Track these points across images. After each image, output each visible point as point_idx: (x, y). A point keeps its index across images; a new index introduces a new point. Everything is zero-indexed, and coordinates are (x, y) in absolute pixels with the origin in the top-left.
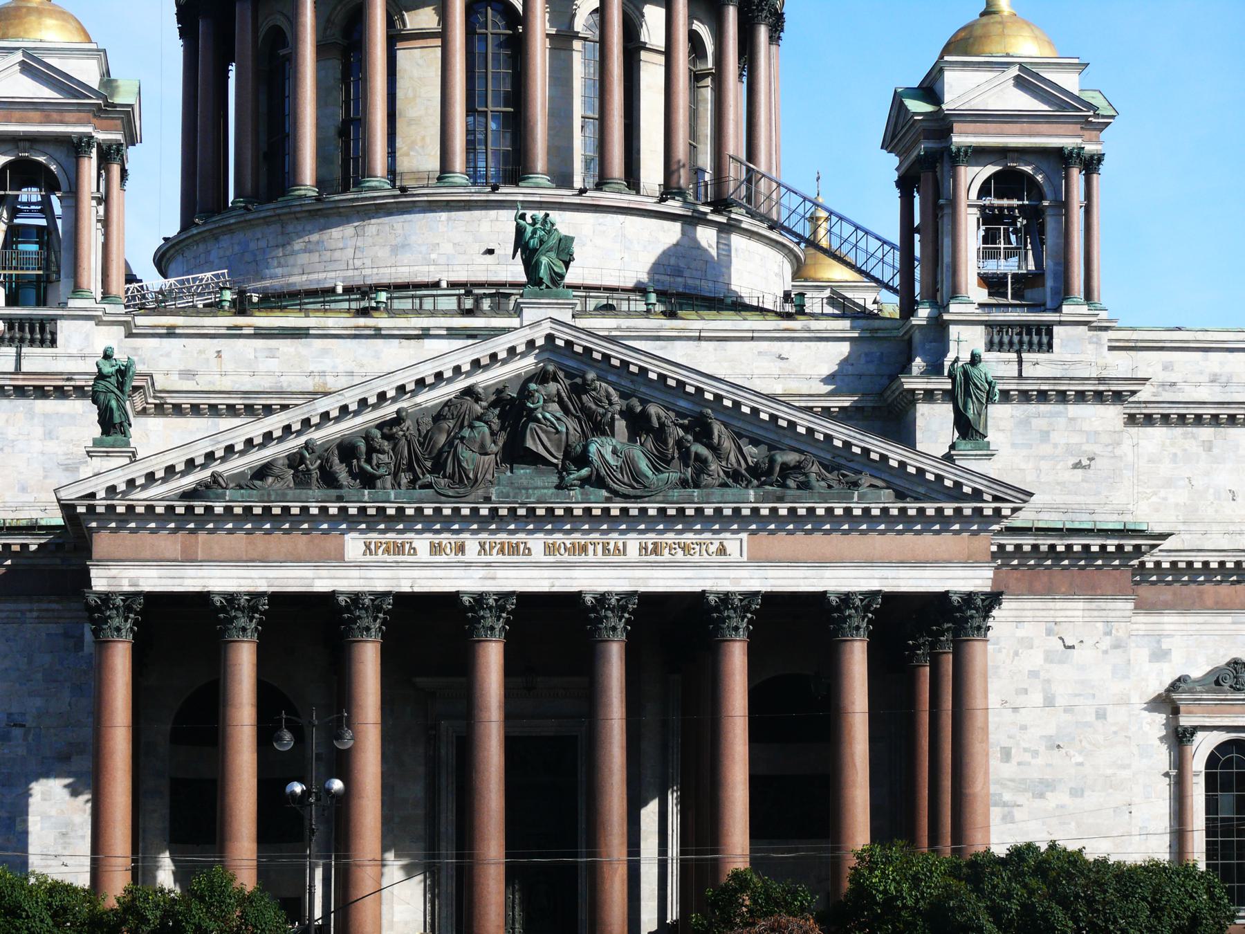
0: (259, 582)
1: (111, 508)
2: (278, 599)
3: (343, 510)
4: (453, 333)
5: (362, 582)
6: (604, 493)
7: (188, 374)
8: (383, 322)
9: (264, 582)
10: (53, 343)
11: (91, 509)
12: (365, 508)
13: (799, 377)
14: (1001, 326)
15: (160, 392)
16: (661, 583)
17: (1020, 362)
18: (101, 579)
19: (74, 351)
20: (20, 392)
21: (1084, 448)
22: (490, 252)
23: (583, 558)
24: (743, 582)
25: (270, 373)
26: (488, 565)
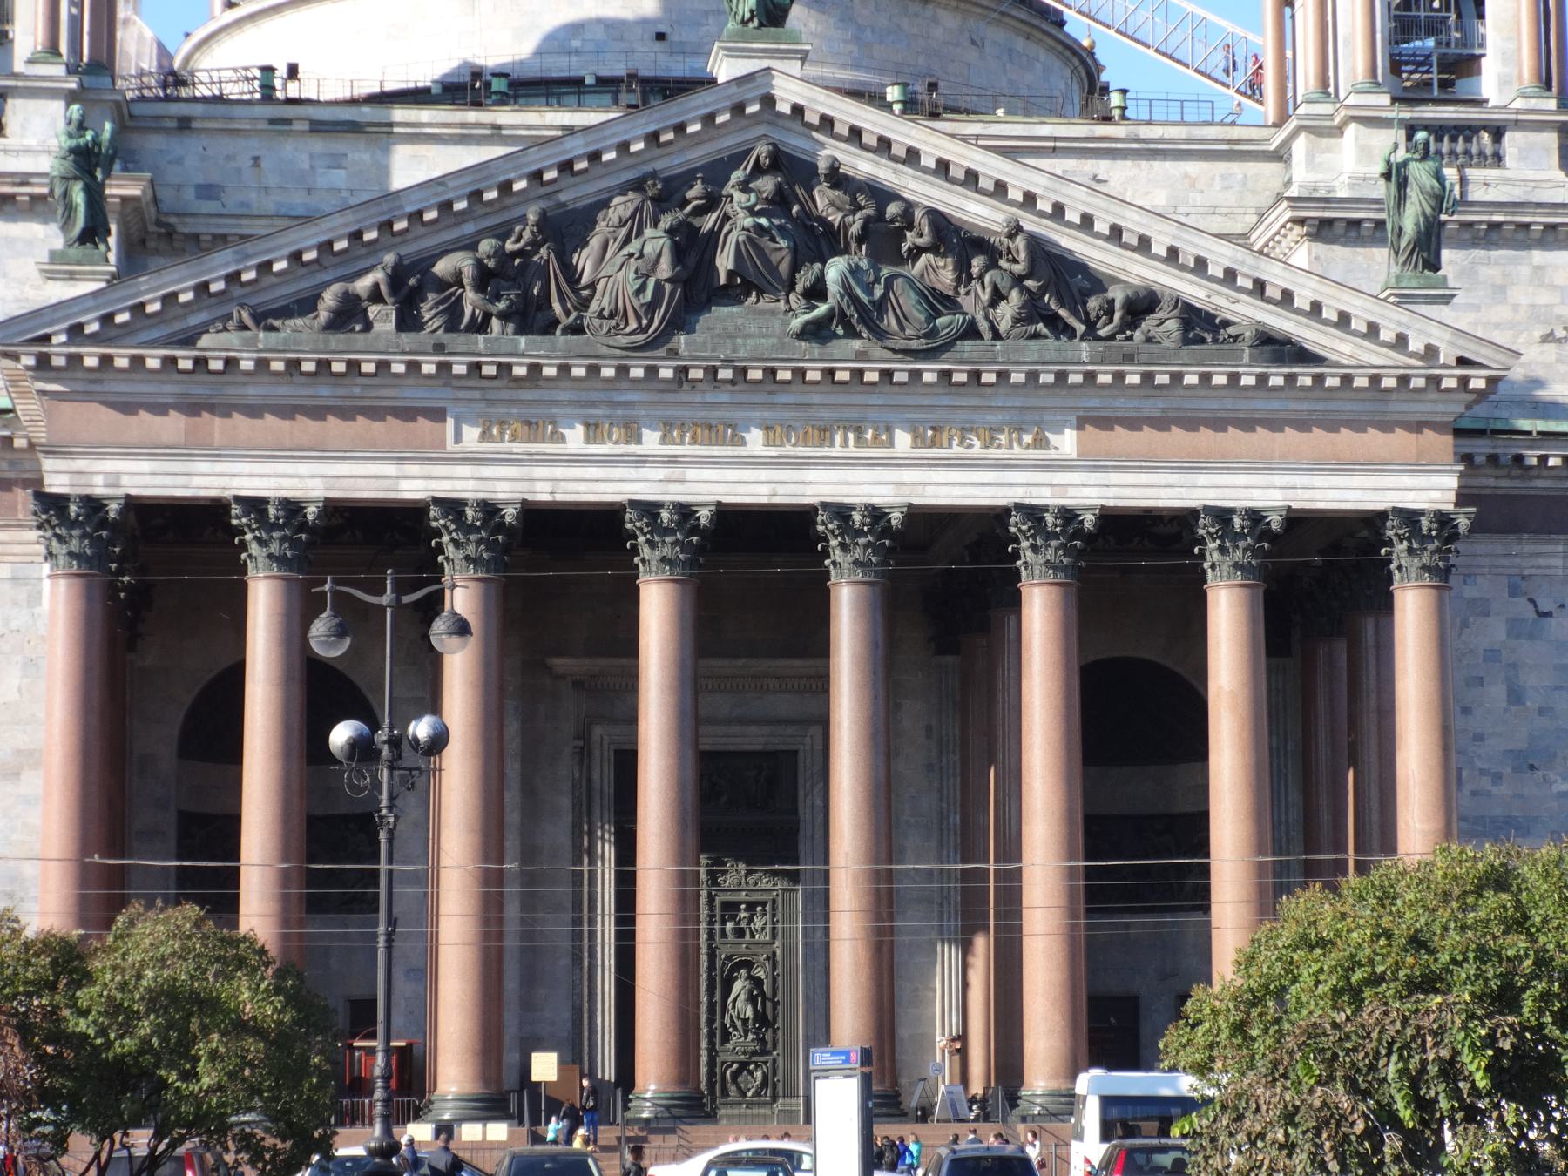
0: (311, 483)
1: (74, 360)
3: (444, 367)
5: (471, 485)
6: (856, 344)
7: (208, 191)
9: (318, 483)
11: (43, 362)
12: (478, 366)
14: (1439, 130)
15: (167, 214)
16: (943, 491)
17: (1463, 181)
19: (31, 141)
21: (1559, 311)
22: (661, 37)
24: (1072, 492)
26: (673, 460)
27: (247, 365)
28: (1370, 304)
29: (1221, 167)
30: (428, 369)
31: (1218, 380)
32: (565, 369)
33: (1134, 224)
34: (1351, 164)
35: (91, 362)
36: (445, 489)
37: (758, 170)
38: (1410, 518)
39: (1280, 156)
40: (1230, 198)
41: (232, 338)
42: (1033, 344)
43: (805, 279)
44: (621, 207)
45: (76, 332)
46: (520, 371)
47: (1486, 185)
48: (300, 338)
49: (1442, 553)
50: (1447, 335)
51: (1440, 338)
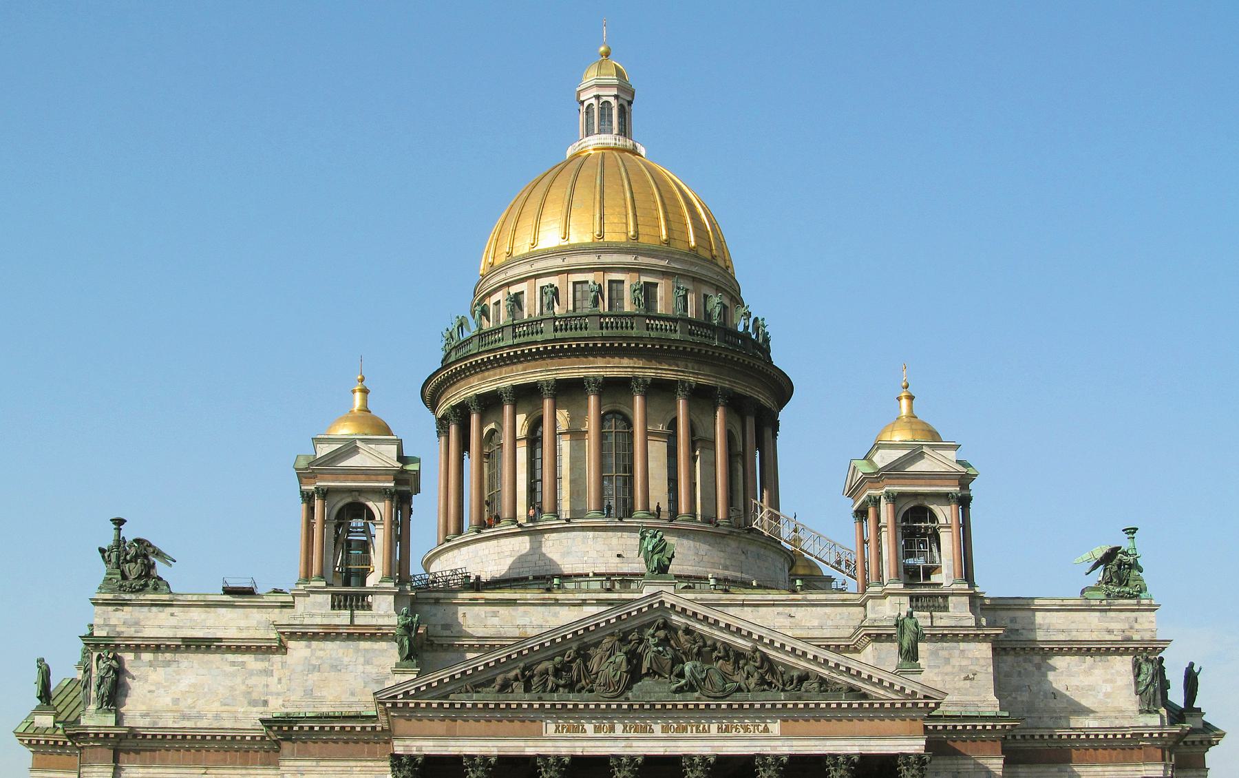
2: (502, 759)
3: (542, 705)
4: (600, 602)
7: (447, 627)
8: (560, 596)
10: (369, 607)
11: (395, 705)
13: (802, 628)
17: (932, 617)
18: (399, 748)
20: (350, 637)
22: (619, 556)
23: (684, 734)
25: (494, 626)
26: (627, 739)
27: (469, 706)
28: (891, 676)
29: (839, 609)
30: (536, 706)
31: (834, 706)
32: (587, 706)
33: (801, 646)
34: (889, 609)
35: (412, 705)
36: (542, 751)
37: (658, 628)
38: (906, 756)
39: (865, 606)
40: (843, 622)
41: (464, 696)
42: (763, 694)
43: (677, 669)
44: (607, 642)
45: (406, 694)
46: (570, 707)
47: (943, 620)
48: (489, 696)
49: (921, 770)
50: (919, 687)
51: (917, 688)
